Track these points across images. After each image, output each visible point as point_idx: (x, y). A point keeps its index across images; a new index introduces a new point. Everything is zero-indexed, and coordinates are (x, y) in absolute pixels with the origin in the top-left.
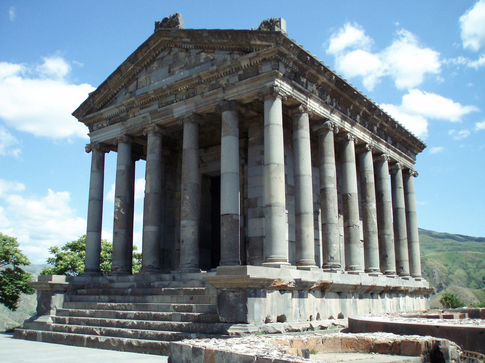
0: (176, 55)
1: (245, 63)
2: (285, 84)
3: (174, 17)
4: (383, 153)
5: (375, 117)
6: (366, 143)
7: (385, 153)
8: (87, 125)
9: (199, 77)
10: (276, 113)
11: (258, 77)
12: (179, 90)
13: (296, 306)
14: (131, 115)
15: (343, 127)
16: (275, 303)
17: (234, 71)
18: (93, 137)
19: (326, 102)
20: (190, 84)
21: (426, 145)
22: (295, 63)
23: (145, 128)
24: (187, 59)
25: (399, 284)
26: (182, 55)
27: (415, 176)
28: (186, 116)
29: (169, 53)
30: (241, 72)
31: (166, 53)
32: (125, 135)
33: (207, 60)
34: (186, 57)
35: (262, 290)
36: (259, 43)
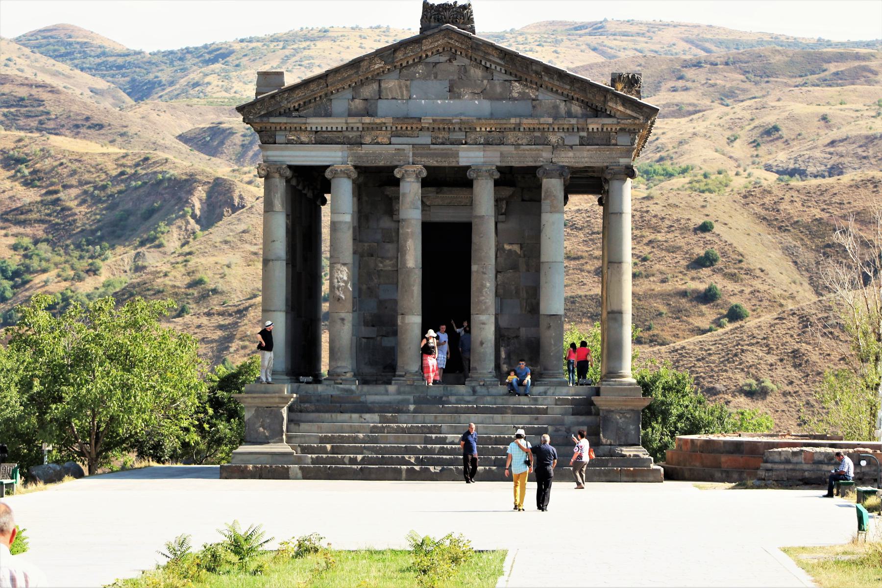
0: (464, 70)
3: (464, 7)
9: (520, 124)
12: (478, 129)
14: (368, 139)
17: (576, 130)
18: (269, 153)
20: (499, 126)
23: (396, 167)
24: (485, 82)
26: (477, 73)
28: (484, 169)
29: (450, 60)
30: (584, 134)
31: (443, 59)
32: (356, 167)
33: (523, 97)
34: (484, 78)
36: (621, 108)
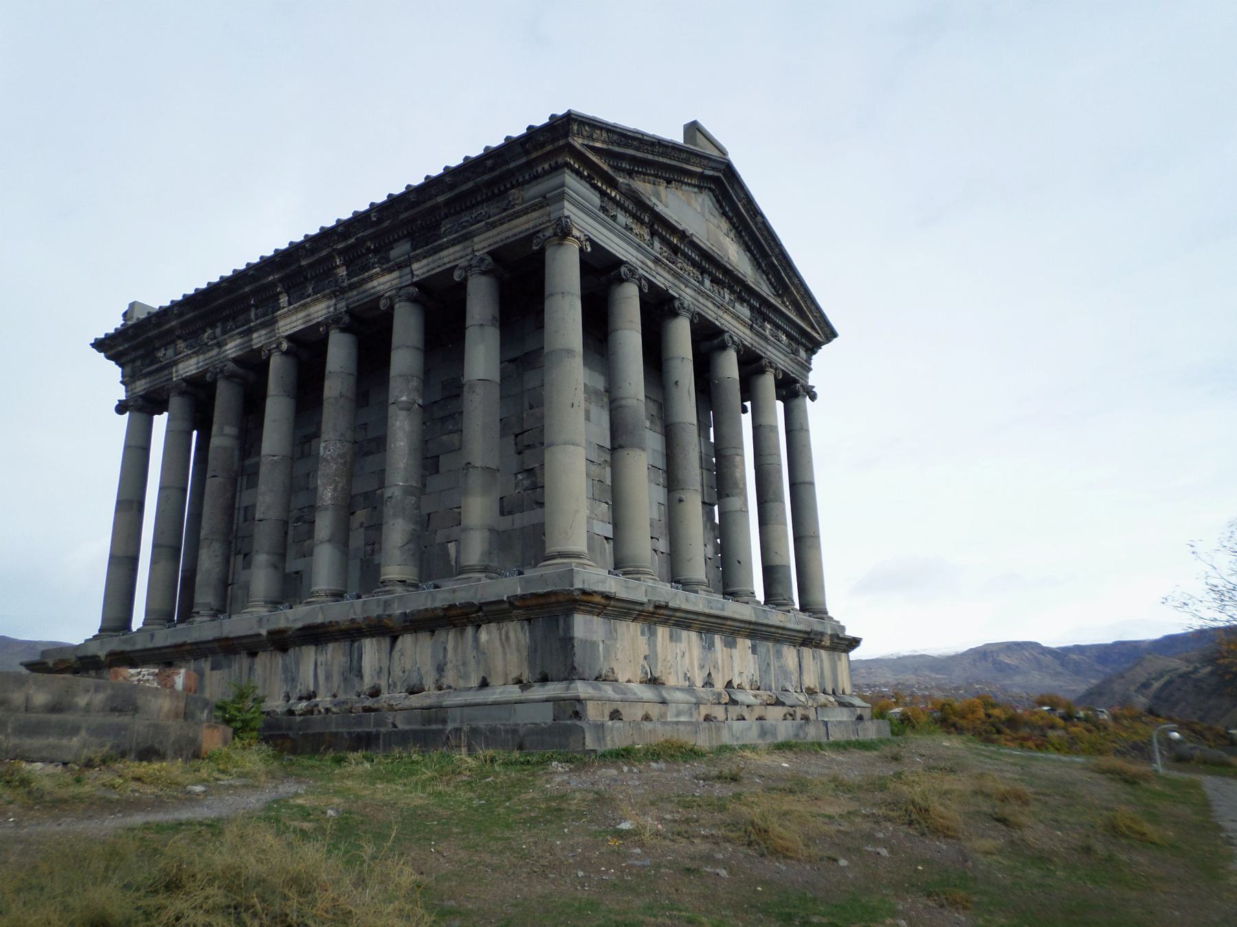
2: (138, 383)
5: (303, 263)
22: (135, 348)
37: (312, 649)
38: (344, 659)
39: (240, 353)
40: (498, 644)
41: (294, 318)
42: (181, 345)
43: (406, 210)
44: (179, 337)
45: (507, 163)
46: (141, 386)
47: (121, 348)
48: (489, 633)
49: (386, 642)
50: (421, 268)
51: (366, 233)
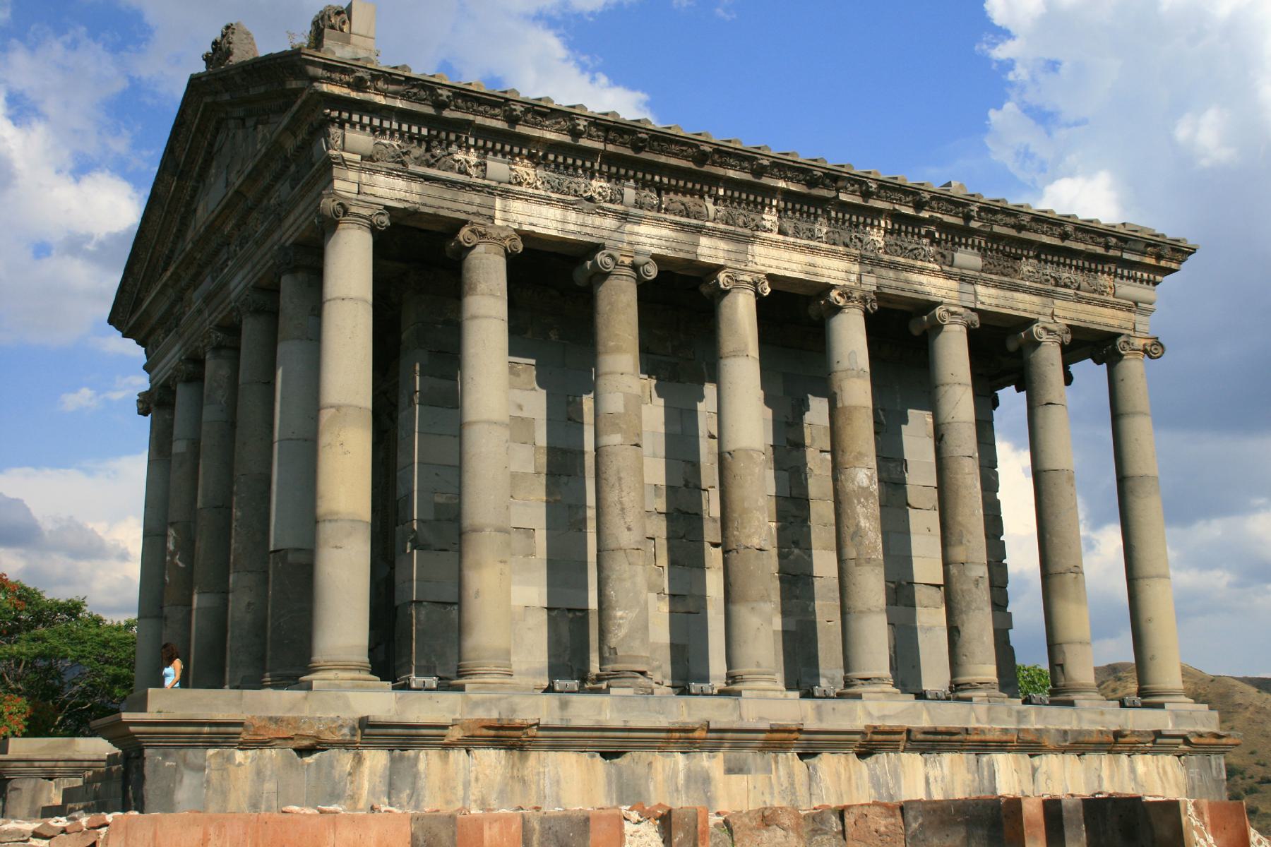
1: (290, 145)
2: (380, 179)
4: (936, 304)
5: (843, 197)
6: (833, 287)
7: (941, 303)
8: (141, 342)
10: (351, 266)
11: (313, 177)
13: (372, 792)
15: (688, 256)
16: (270, 786)
18: (154, 372)
19: (591, 199)
21: (1191, 242)
22: (403, 115)
25: (991, 720)
26: (240, 133)
27: (1145, 351)
30: (293, 168)
35: (211, 752)
37: (918, 755)
38: (970, 777)
39: (671, 254)
40: (1156, 777)
41: (786, 255)
42: (524, 169)
43: (1006, 225)
44: (531, 157)
45: (1122, 250)
46: (392, 190)
47: (380, 100)
48: (1146, 764)
49: (1024, 759)
50: (989, 297)
51: (947, 219)
